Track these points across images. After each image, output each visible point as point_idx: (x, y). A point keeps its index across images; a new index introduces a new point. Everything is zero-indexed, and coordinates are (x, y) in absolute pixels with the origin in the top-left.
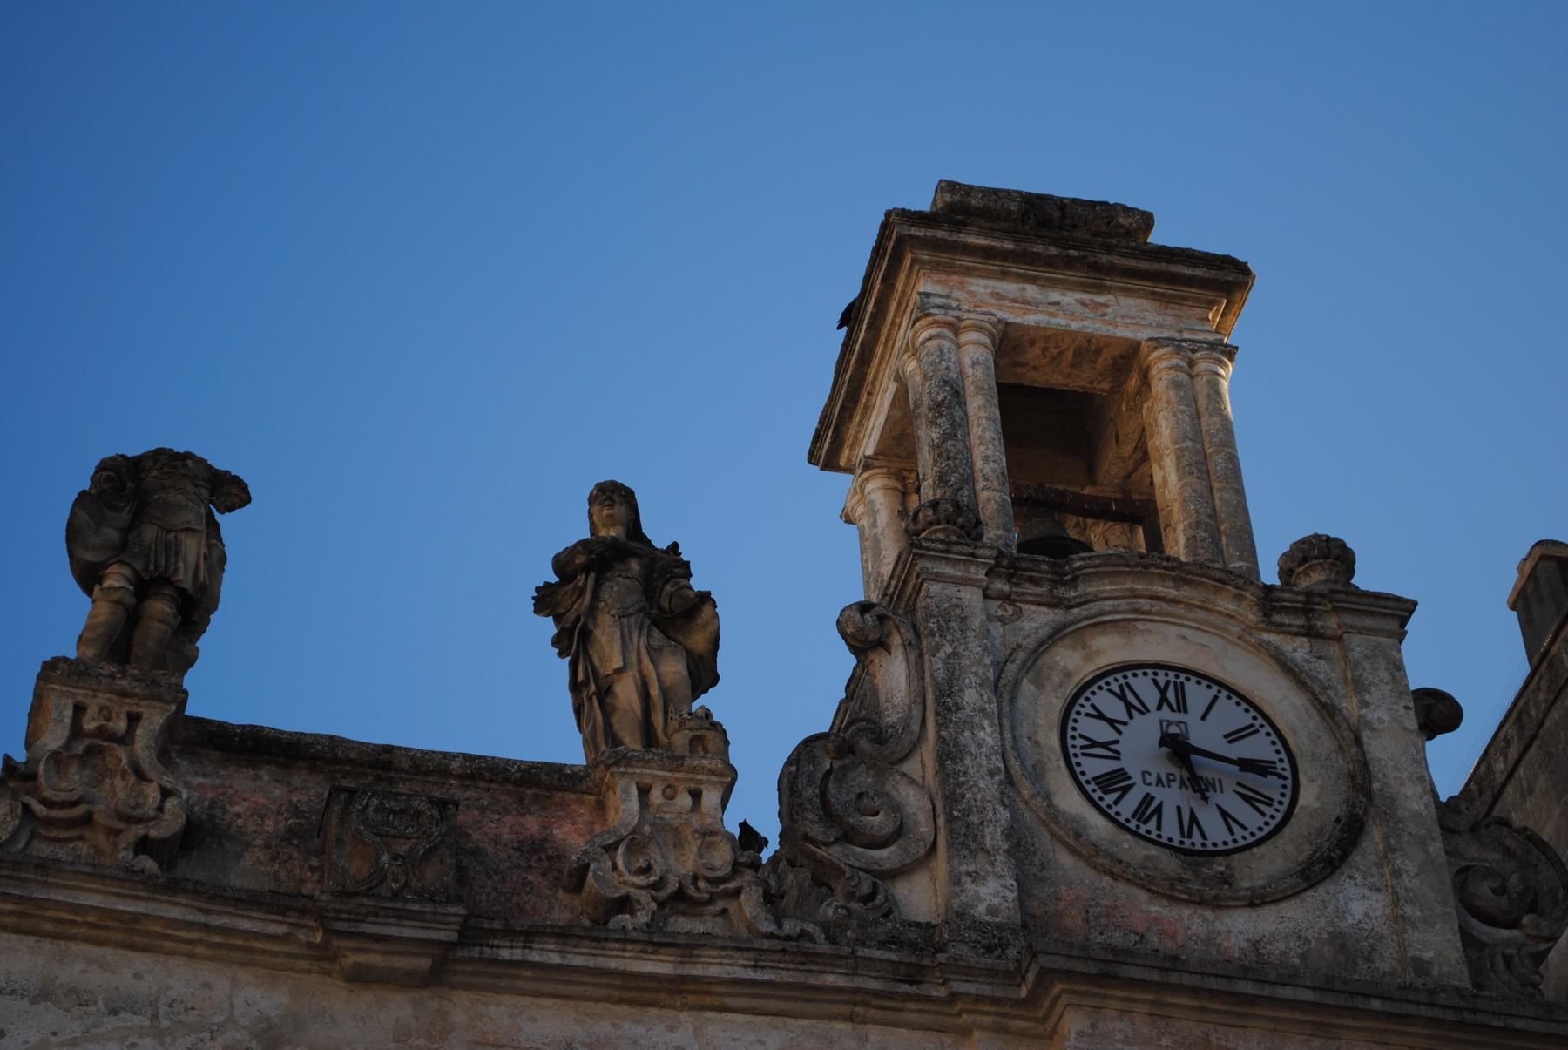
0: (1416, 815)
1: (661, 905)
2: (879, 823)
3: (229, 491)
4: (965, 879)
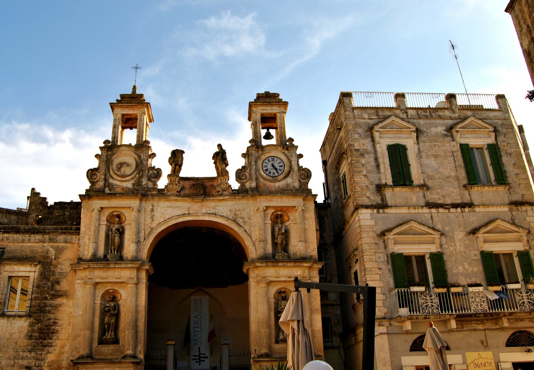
2: (244, 178)
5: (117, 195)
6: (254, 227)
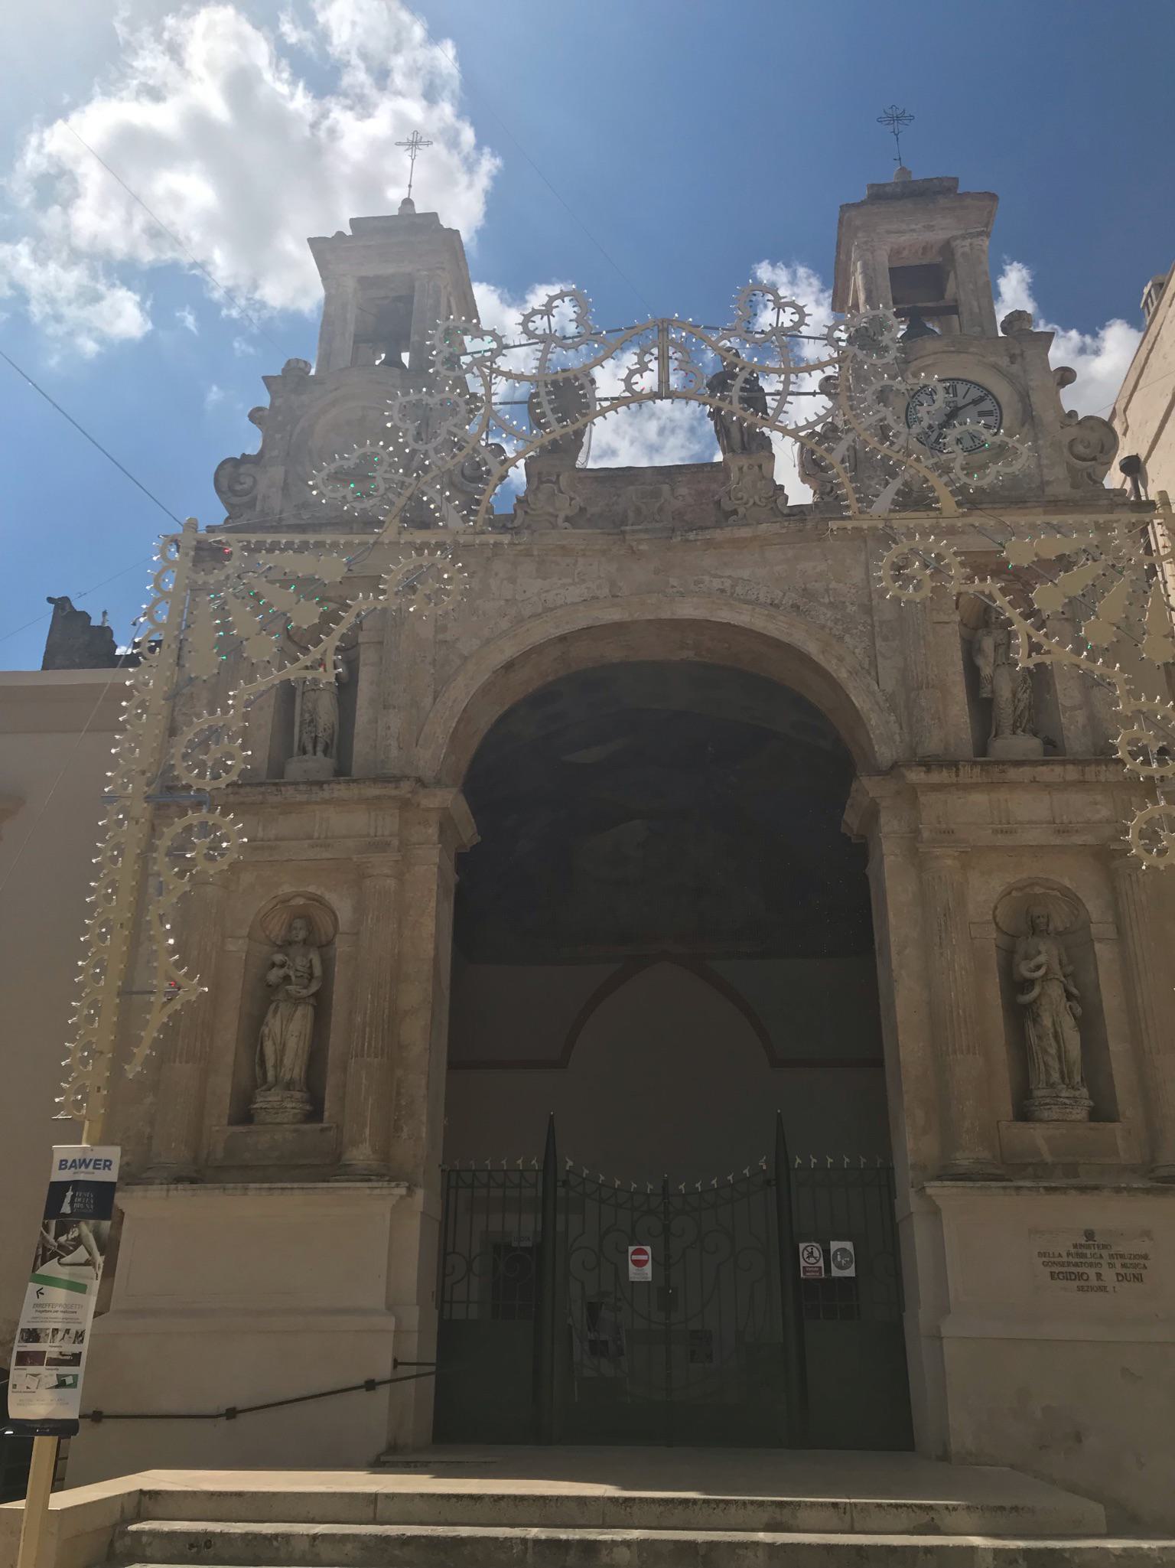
6: (885, 639)
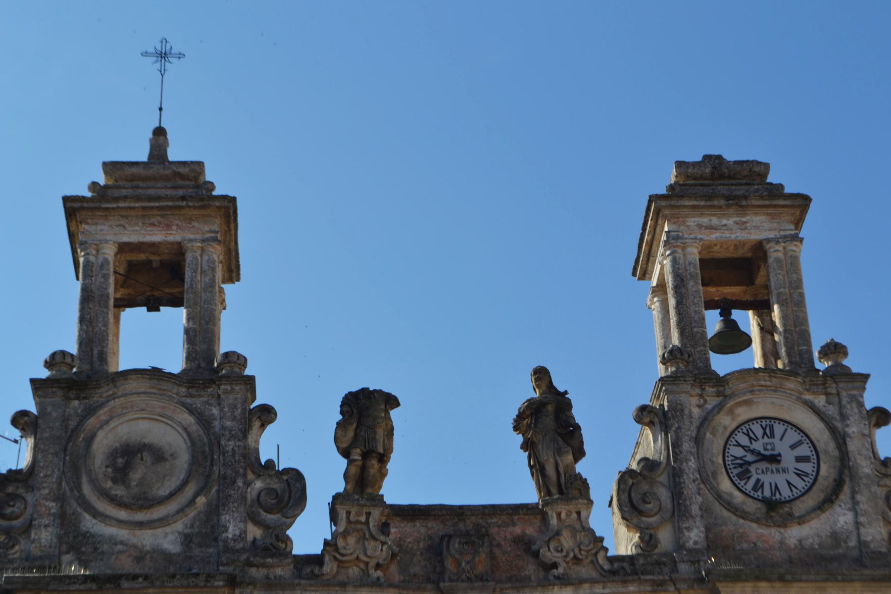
0: (867, 476)
1: (567, 563)
3: (392, 401)
4: (685, 531)
5: (125, 584)
